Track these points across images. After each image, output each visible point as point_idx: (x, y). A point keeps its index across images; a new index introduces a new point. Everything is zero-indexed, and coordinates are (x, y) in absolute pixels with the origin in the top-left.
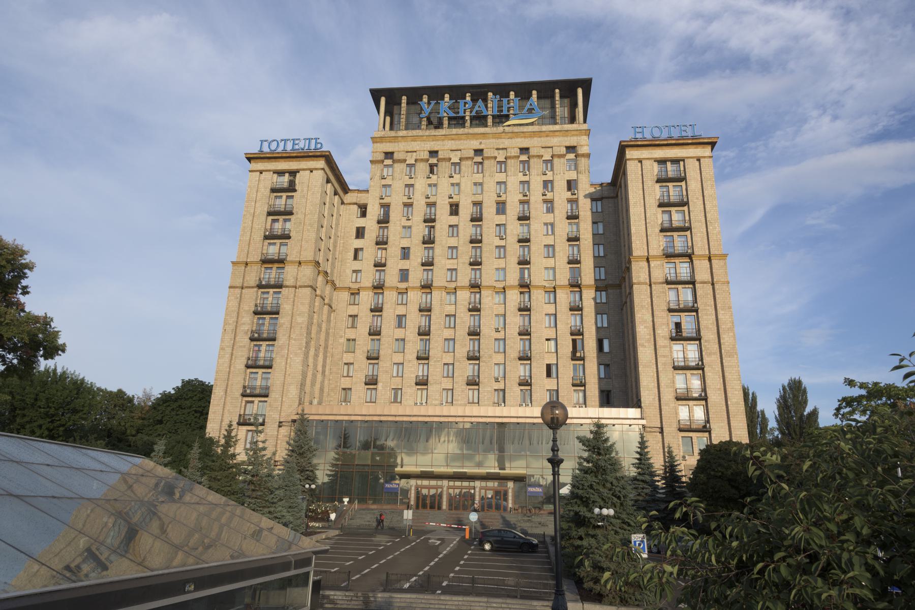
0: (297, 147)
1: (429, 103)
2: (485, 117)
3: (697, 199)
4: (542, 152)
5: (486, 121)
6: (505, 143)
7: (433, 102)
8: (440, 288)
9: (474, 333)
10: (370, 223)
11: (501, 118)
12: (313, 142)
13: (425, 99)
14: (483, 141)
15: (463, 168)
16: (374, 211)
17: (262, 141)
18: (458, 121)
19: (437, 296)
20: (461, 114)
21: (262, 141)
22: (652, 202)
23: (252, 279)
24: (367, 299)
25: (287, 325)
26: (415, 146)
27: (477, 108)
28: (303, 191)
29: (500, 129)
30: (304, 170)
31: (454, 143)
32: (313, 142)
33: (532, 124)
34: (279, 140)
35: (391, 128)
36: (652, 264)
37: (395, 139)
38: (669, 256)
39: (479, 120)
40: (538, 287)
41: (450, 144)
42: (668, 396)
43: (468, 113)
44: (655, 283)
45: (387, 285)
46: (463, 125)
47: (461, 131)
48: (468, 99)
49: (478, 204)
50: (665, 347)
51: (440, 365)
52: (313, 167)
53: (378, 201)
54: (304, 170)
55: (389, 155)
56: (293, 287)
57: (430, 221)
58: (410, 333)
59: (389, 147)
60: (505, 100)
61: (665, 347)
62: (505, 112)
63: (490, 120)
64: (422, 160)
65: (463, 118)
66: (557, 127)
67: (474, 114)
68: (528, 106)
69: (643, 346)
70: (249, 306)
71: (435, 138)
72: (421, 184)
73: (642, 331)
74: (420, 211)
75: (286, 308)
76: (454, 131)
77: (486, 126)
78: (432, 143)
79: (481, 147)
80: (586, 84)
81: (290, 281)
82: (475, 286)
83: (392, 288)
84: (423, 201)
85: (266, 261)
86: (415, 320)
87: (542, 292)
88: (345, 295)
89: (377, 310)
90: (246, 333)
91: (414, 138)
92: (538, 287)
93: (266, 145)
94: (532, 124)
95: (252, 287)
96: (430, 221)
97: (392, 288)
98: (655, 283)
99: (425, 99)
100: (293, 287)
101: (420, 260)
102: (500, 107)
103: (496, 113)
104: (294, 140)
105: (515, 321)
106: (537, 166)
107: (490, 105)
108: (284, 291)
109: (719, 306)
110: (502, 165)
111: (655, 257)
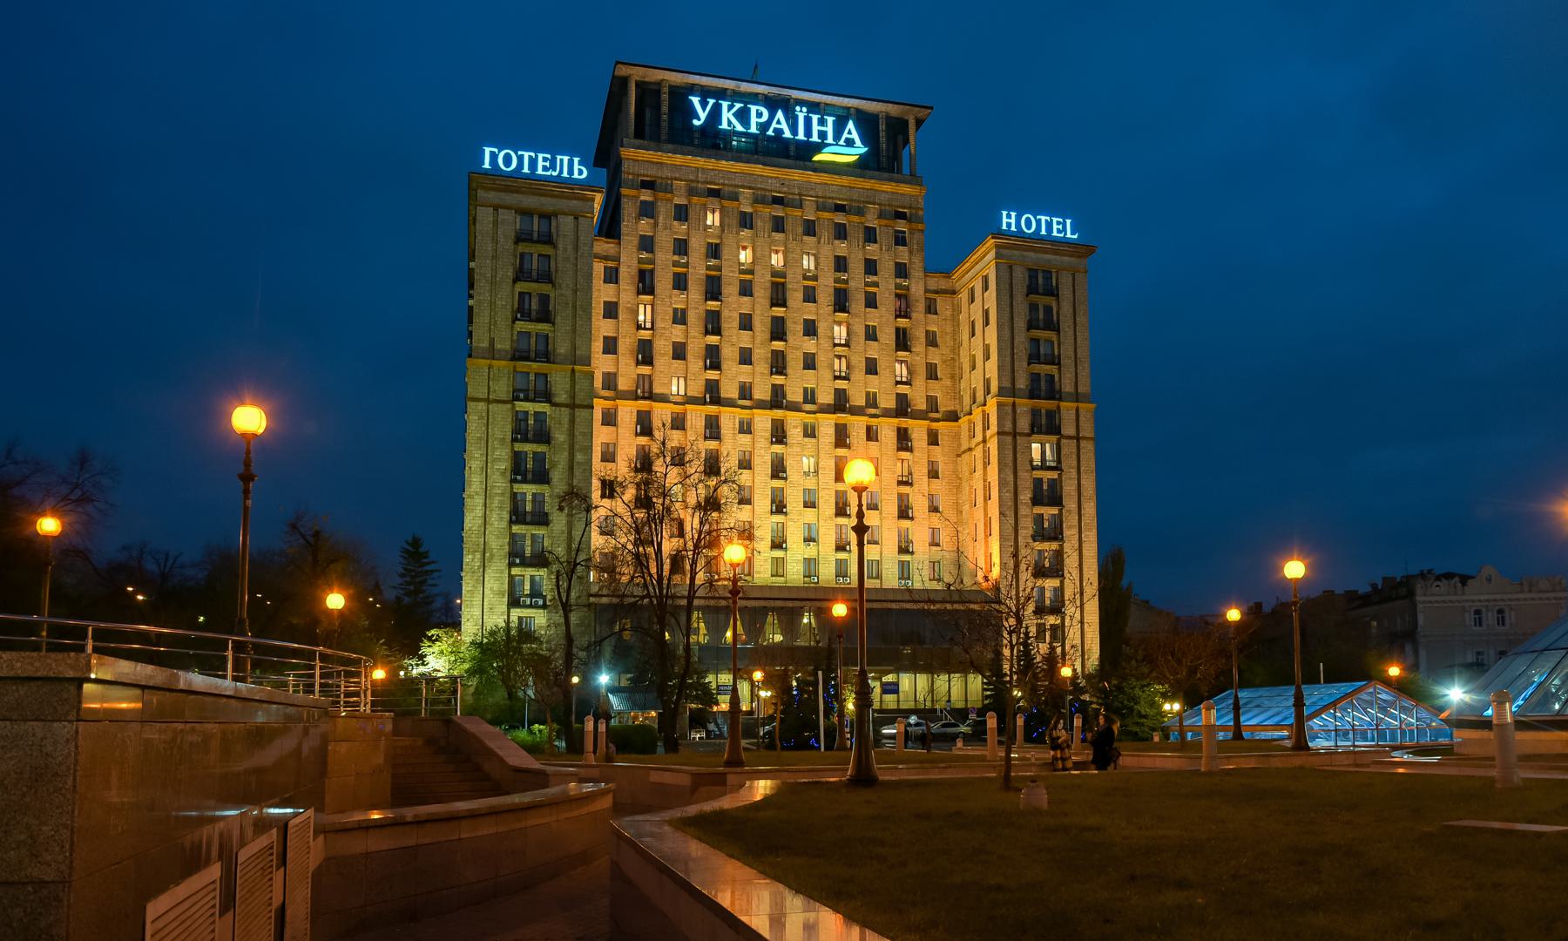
1: (704, 104)
7: (711, 102)
27: (774, 125)
28: (565, 250)
68: (845, 135)
102: (808, 132)
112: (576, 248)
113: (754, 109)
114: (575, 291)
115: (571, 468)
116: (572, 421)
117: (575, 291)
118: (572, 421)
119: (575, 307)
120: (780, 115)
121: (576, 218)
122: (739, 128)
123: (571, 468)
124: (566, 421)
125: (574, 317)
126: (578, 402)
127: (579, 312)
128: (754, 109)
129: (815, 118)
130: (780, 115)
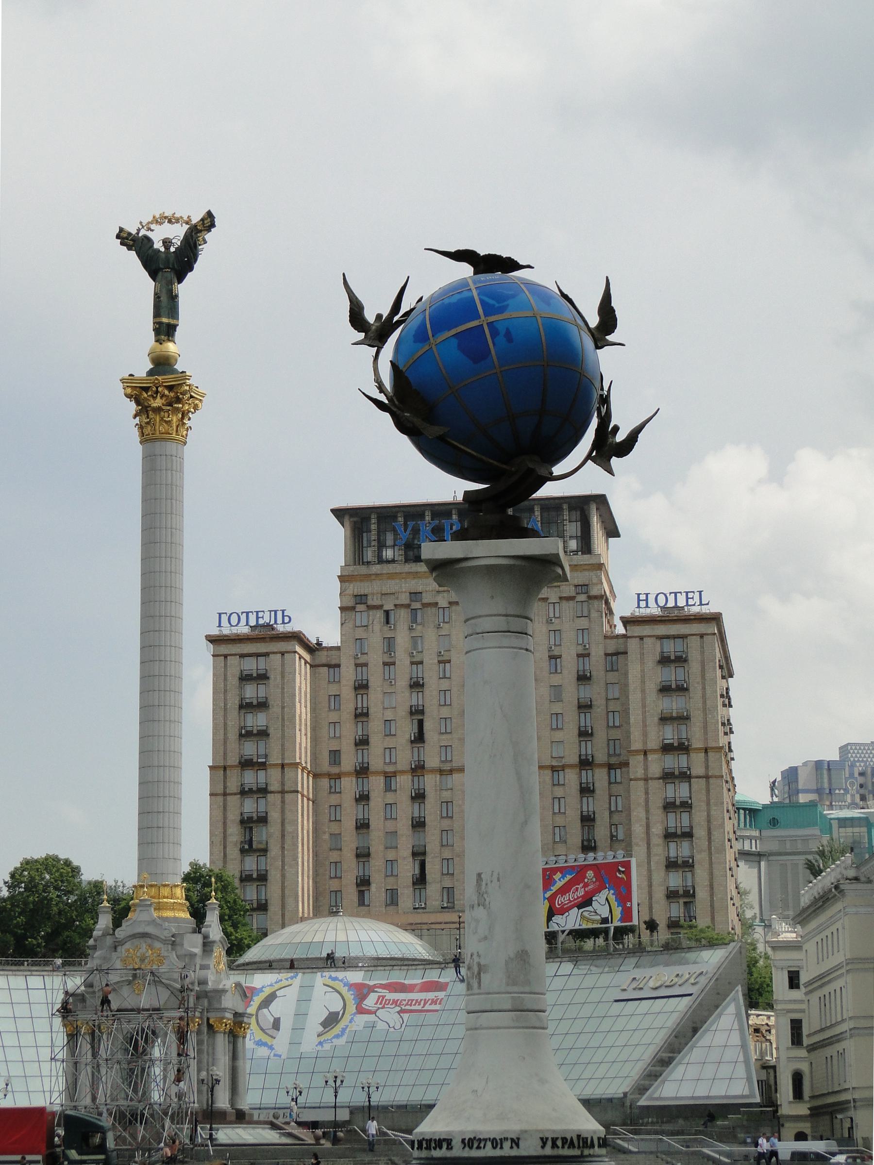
0: (261, 622)
3: (698, 683)
7: (411, 524)
8: (433, 771)
10: (347, 692)
12: (279, 614)
15: (454, 617)
17: (220, 614)
19: (430, 782)
21: (220, 614)
22: (652, 687)
23: (233, 785)
24: (349, 786)
25: (278, 834)
26: (391, 586)
28: (275, 678)
30: (274, 653)
32: (279, 614)
34: (239, 612)
36: (650, 757)
37: (367, 577)
38: (667, 749)
42: (659, 894)
44: (651, 779)
45: (372, 768)
50: (658, 845)
51: (438, 861)
52: (283, 650)
53: (352, 662)
54: (274, 653)
55: (361, 599)
56: (279, 792)
57: (417, 685)
58: (404, 826)
61: (658, 845)
64: (402, 606)
69: (637, 845)
70: (233, 816)
72: (402, 639)
73: (638, 829)
74: (403, 673)
75: (274, 816)
78: (413, 582)
80: (601, 500)
81: (275, 786)
83: (377, 773)
85: (246, 764)
86: (406, 810)
88: (325, 783)
89: (363, 798)
90: (235, 844)
91: (391, 576)
93: (224, 618)
95: (235, 794)
96: (417, 685)
97: (377, 773)
98: (651, 779)
99: (401, 519)
100: (279, 792)
101: (408, 736)
104: (257, 612)
108: (270, 797)
109: (712, 801)
111: (654, 751)
112: (283, 677)
114: (283, 708)
115: (283, 836)
116: (283, 802)
117: (283, 708)
118: (283, 802)
119: (283, 719)
121: (283, 655)
123: (283, 836)
124: (279, 802)
125: (283, 726)
126: (286, 789)
127: (286, 723)
128: (446, 523)
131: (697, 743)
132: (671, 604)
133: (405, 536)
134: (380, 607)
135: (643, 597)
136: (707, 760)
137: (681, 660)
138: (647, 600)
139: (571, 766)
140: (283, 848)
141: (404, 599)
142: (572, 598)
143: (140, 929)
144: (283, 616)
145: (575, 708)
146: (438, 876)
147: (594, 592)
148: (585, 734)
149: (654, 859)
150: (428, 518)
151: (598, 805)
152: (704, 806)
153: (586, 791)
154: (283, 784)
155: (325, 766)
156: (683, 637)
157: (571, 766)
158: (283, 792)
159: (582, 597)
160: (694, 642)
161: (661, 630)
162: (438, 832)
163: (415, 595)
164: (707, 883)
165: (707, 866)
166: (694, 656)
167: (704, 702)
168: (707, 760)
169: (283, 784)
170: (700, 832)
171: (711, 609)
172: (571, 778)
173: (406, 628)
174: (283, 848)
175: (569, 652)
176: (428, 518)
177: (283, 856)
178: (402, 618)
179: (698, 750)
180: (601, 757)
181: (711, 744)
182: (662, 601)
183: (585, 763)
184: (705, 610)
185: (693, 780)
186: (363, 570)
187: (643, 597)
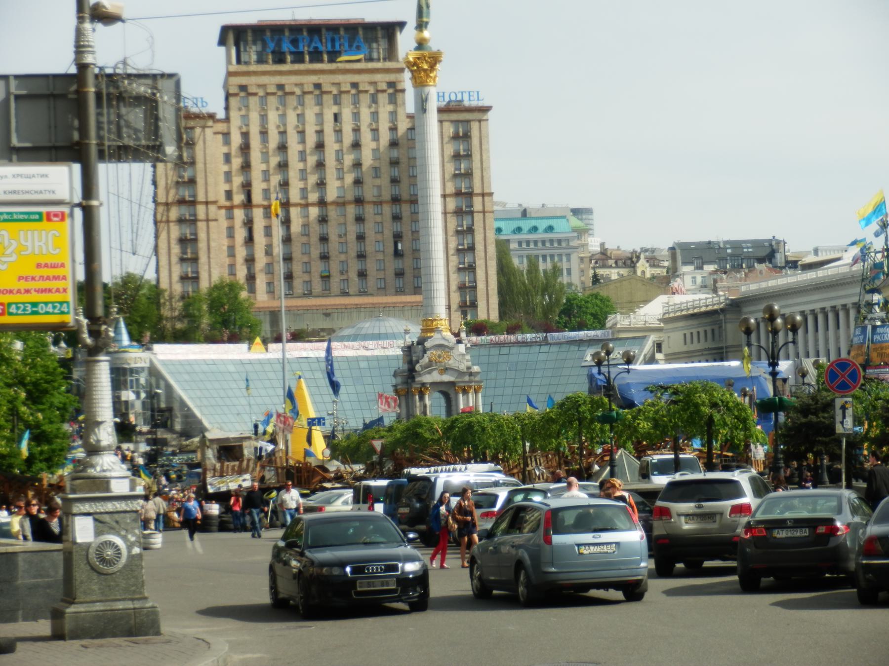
2: (321, 53)
4: (367, 87)
5: (322, 56)
6: (339, 78)
7: (276, 37)
9: (324, 239)
11: (333, 56)
13: (268, 34)
14: (322, 76)
16: (236, 139)
18: (298, 58)
20: (301, 49)
26: (265, 80)
27: (313, 45)
29: (333, 66)
31: (296, 76)
33: (359, 61)
35: (239, 61)
39: (316, 56)
40: (369, 203)
41: (294, 79)
43: (306, 48)
46: (302, 61)
47: (301, 67)
48: (305, 34)
49: (320, 132)
59: (243, 81)
60: (336, 37)
62: (337, 48)
63: (325, 57)
65: (302, 53)
66: (379, 65)
67: (311, 49)
71: (281, 73)
72: (273, 117)
76: (297, 67)
77: (322, 61)
79: (321, 81)
82: (322, 203)
84: (276, 132)
87: (372, 206)
91: (264, 73)
92: (369, 203)
94: (359, 61)
96: (283, 148)
97: (258, 206)
102: (333, 46)
103: (330, 48)
105: (353, 230)
106: (365, 99)
107: (324, 41)
110: (337, 101)
113: (299, 37)
120: (316, 38)
122: (293, 49)
128: (299, 37)
129: (336, 37)
130: (316, 38)
131: (477, 189)
132: (459, 98)
133: (271, 46)
134: (255, 94)
135: (441, 94)
136: (483, 201)
137: (467, 136)
138: (444, 96)
139: (386, 202)
140: (209, 257)
141: (272, 89)
142: (384, 91)
143: (437, 343)
144: (202, 102)
145: (388, 164)
146: (300, 273)
147: (399, 87)
148: (395, 181)
149: (451, 264)
150: (287, 34)
151: (405, 228)
152: (482, 230)
153: (396, 218)
154: (207, 214)
155: (223, 201)
156: (468, 122)
157: (386, 202)
158: (207, 220)
159: (391, 91)
160: (475, 126)
161: (454, 116)
162: (299, 245)
163: (281, 87)
164: (484, 279)
165: (484, 268)
166: (475, 133)
167: (482, 164)
168: (483, 201)
169: (207, 214)
170: (479, 247)
171: (485, 103)
172: (387, 210)
173: (274, 108)
174: (209, 257)
175: (384, 126)
176: (287, 34)
177: (209, 262)
178: (273, 101)
179: (478, 195)
180: (405, 196)
181: (486, 191)
182: (453, 98)
183: (396, 200)
184: (480, 104)
185: (475, 214)
186: (243, 68)
187: (441, 94)
